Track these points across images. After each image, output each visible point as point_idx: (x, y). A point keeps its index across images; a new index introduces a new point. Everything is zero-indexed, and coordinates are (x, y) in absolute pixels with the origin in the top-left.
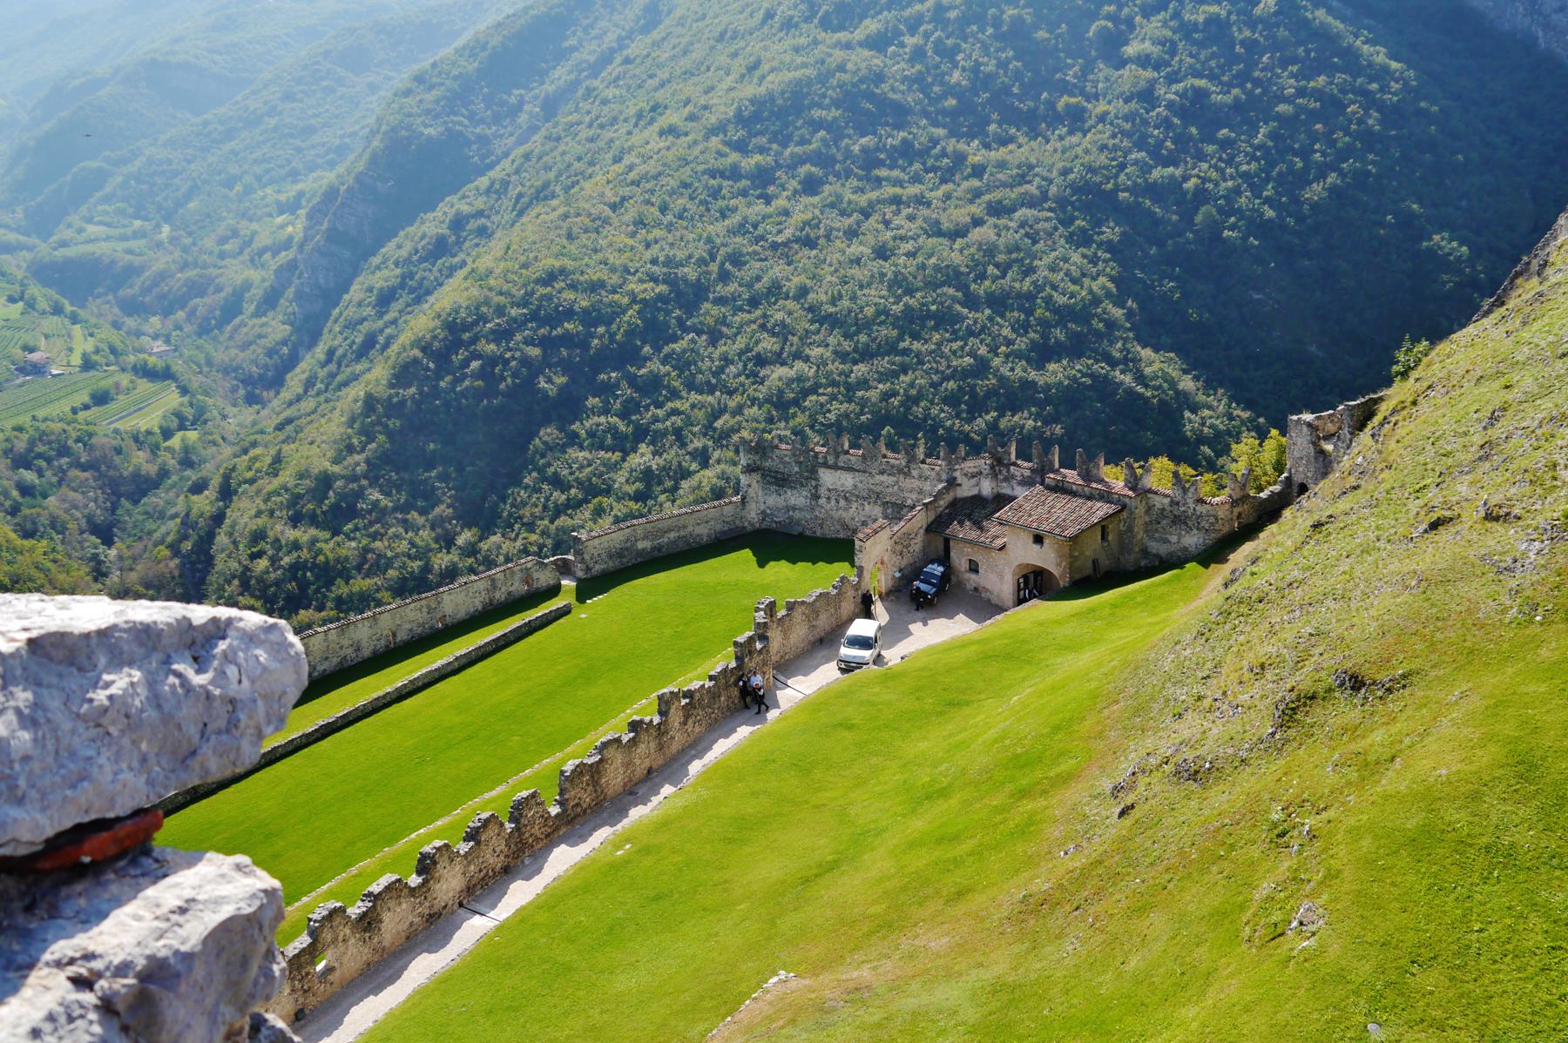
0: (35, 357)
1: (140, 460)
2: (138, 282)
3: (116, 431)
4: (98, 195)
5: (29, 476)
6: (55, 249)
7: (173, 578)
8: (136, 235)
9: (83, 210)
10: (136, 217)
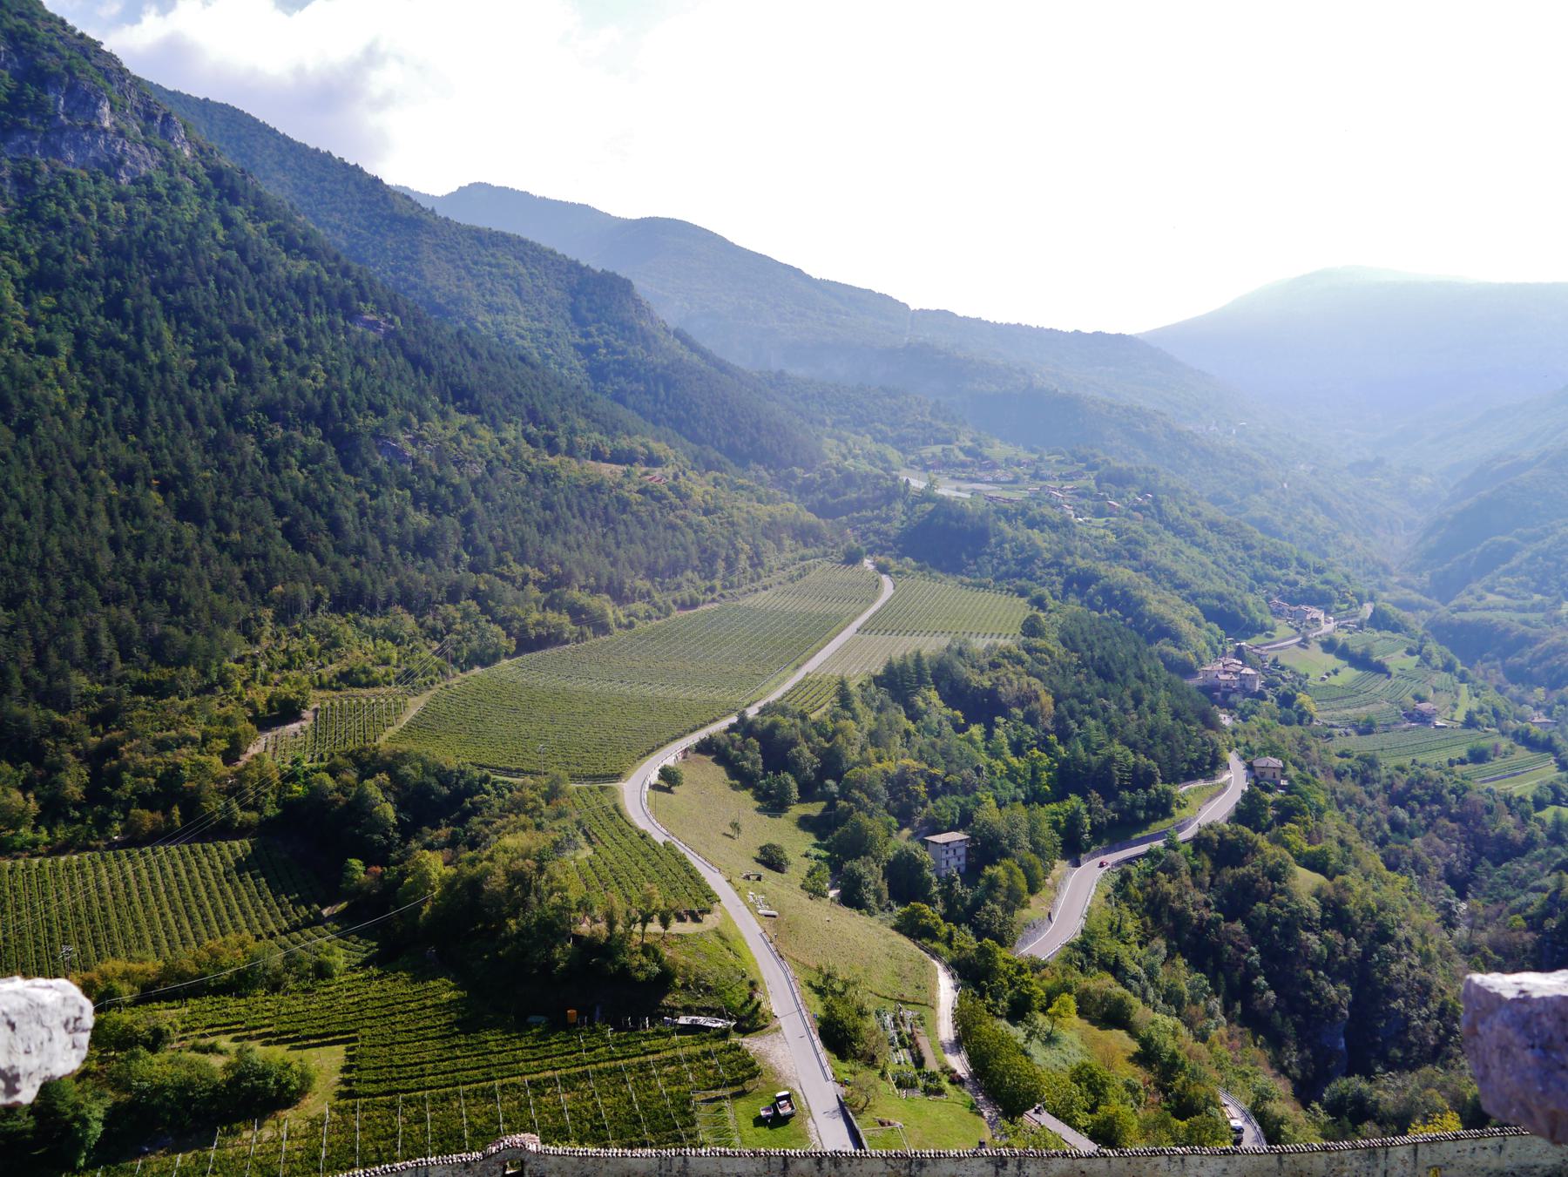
0: (1424, 706)
1: (1508, 822)
2: (1529, 653)
3: (1489, 791)
4: (1503, 567)
5: (1402, 814)
6: (1454, 612)
7: (1525, 951)
8: (1534, 608)
9: (1487, 580)
10: (1537, 591)
